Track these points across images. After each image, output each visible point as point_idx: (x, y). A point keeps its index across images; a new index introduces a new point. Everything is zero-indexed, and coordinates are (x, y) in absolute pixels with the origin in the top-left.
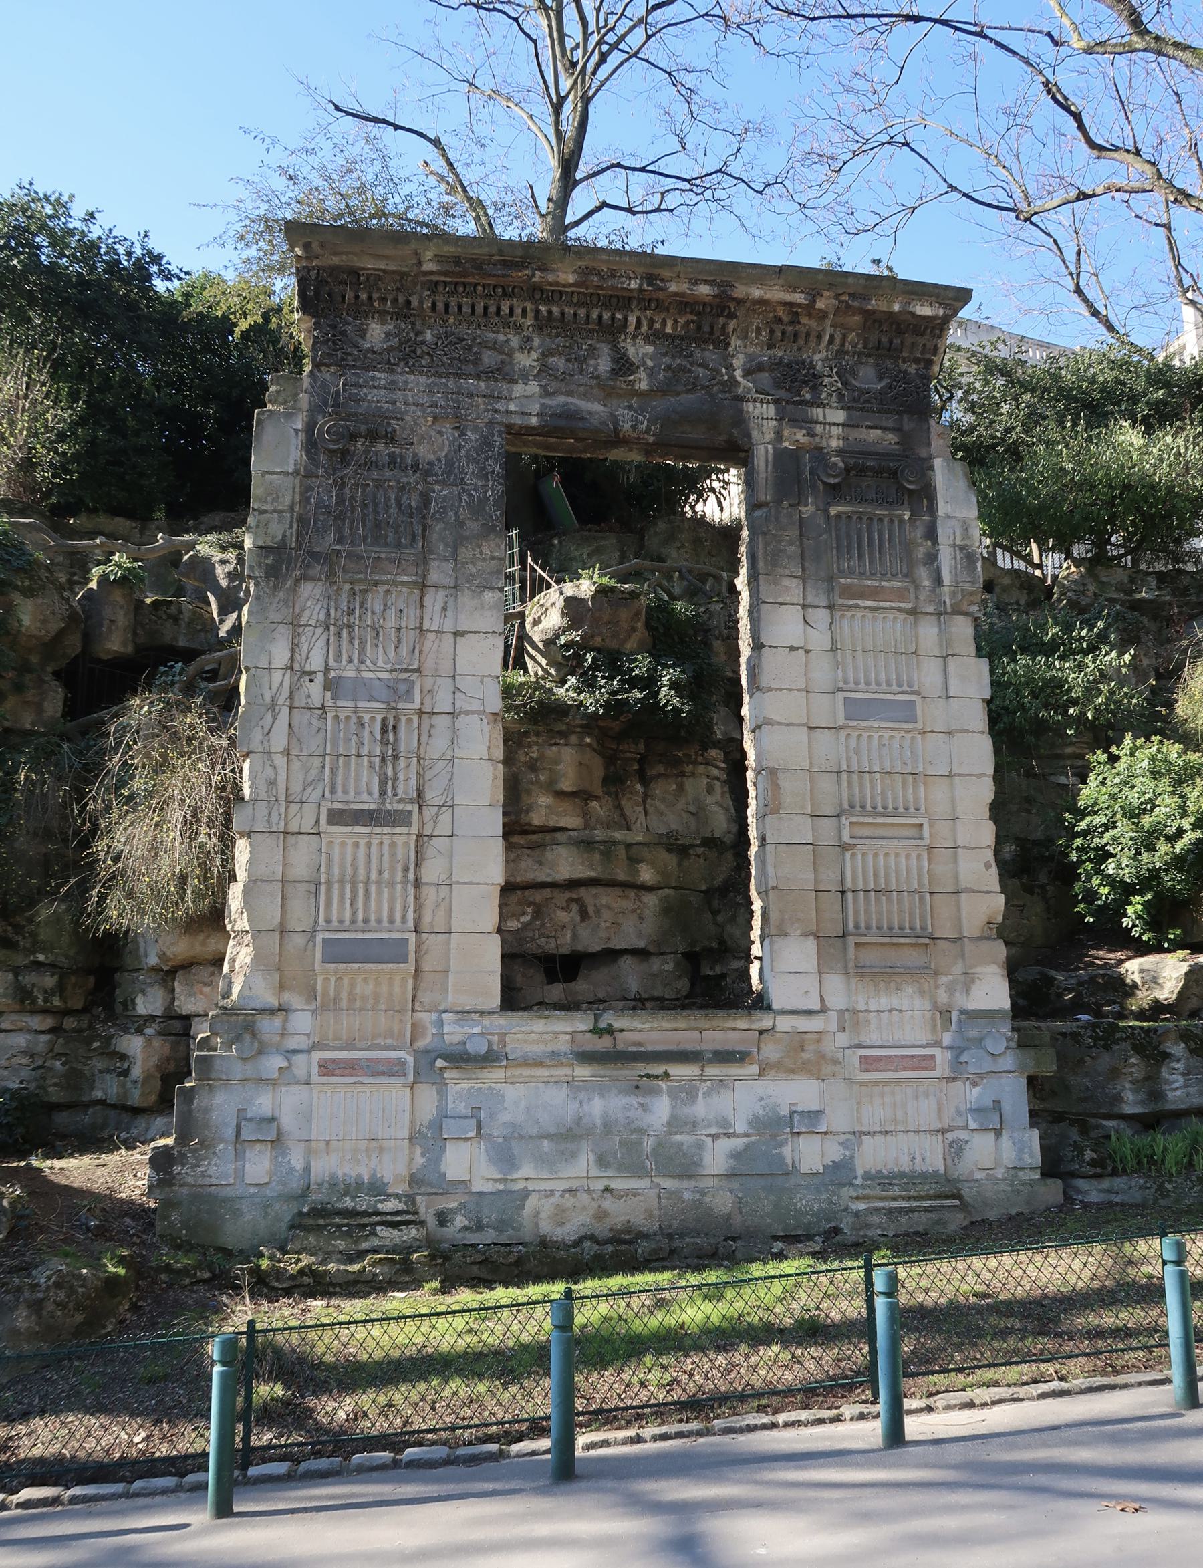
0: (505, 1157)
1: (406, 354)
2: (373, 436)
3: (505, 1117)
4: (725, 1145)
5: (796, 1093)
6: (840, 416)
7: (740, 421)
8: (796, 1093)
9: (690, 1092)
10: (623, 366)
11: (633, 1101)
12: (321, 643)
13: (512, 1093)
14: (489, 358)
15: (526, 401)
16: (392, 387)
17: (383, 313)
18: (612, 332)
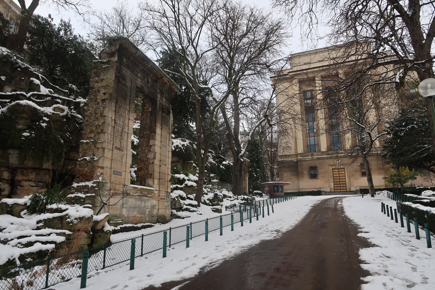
0: (129, 211)
1: (128, 67)
2: (124, 79)
3: (129, 204)
4: (148, 210)
5: (155, 202)
6: (165, 100)
7: (157, 96)
8: (155, 202)
9: (145, 202)
10: (148, 82)
11: (141, 202)
12: (114, 114)
13: (130, 200)
14: (136, 72)
15: (139, 82)
16: (126, 71)
17: (126, 57)
18: (148, 75)
